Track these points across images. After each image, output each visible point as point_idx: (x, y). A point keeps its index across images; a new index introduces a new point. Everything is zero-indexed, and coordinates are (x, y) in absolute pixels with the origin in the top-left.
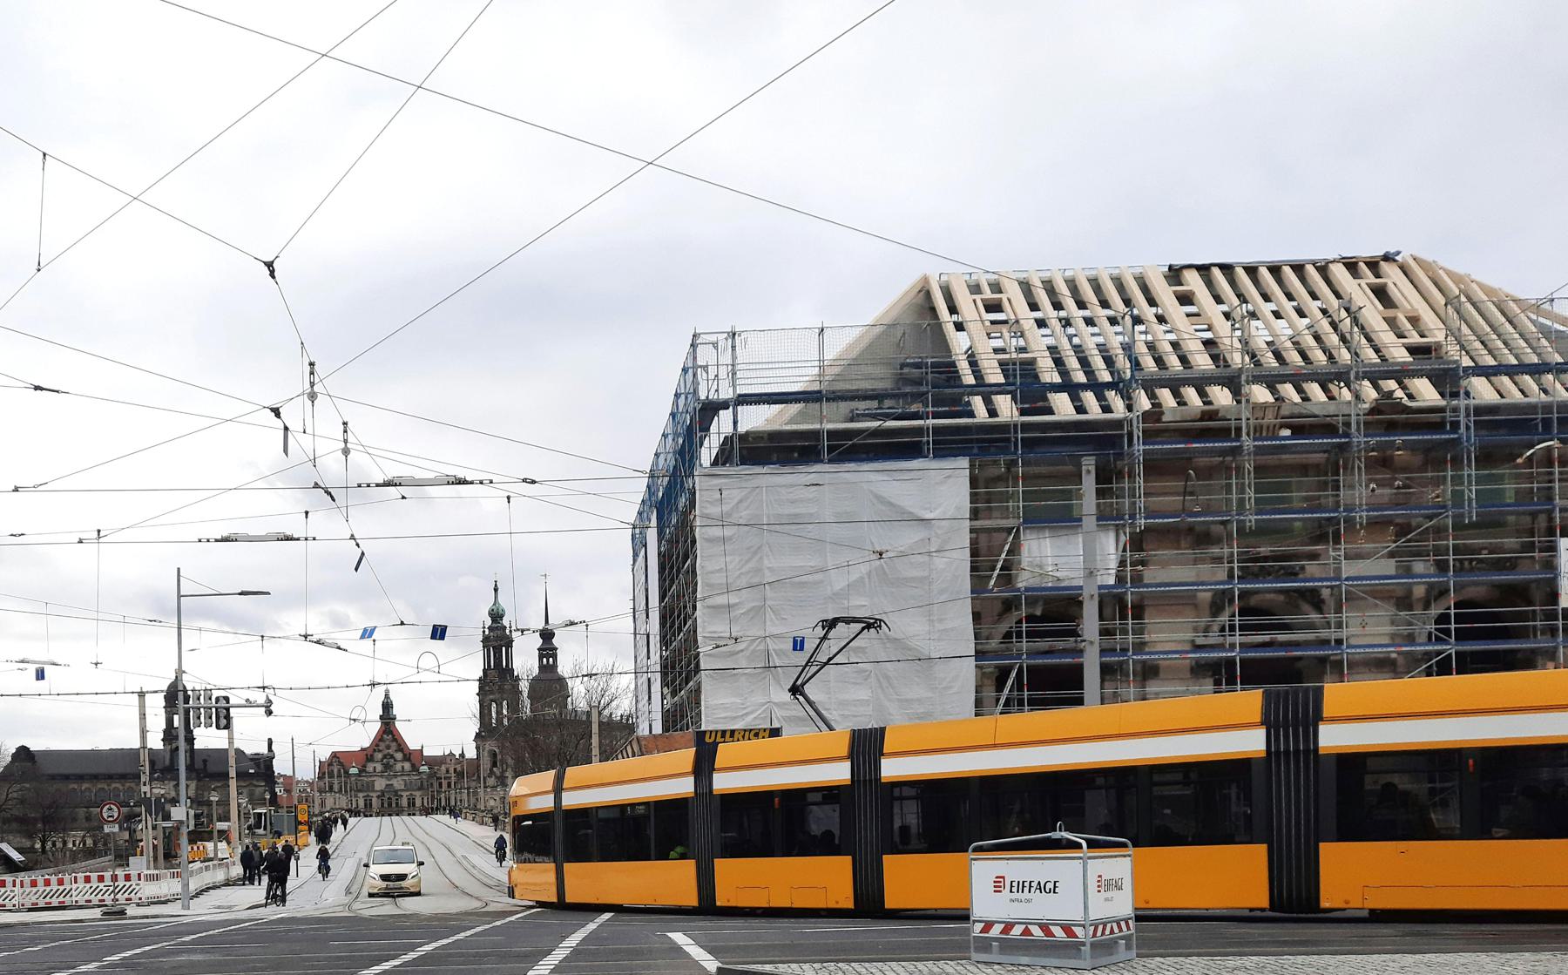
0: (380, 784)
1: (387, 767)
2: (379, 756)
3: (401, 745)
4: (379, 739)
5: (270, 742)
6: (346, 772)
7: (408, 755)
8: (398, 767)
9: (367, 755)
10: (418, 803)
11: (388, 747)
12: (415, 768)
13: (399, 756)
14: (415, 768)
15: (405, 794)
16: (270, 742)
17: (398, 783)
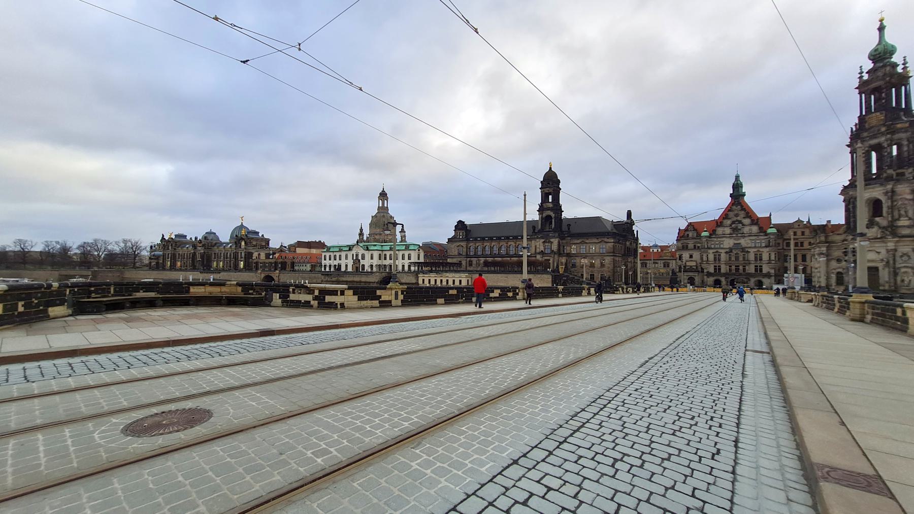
0: (728, 243)
1: (735, 230)
2: (729, 222)
3: (749, 213)
4: (729, 209)
5: (629, 214)
6: (699, 235)
7: (755, 221)
8: (746, 230)
9: (719, 223)
10: (765, 257)
11: (737, 215)
12: (763, 231)
13: (747, 221)
14: (763, 231)
15: (752, 250)
16: (629, 214)
17: (743, 242)
